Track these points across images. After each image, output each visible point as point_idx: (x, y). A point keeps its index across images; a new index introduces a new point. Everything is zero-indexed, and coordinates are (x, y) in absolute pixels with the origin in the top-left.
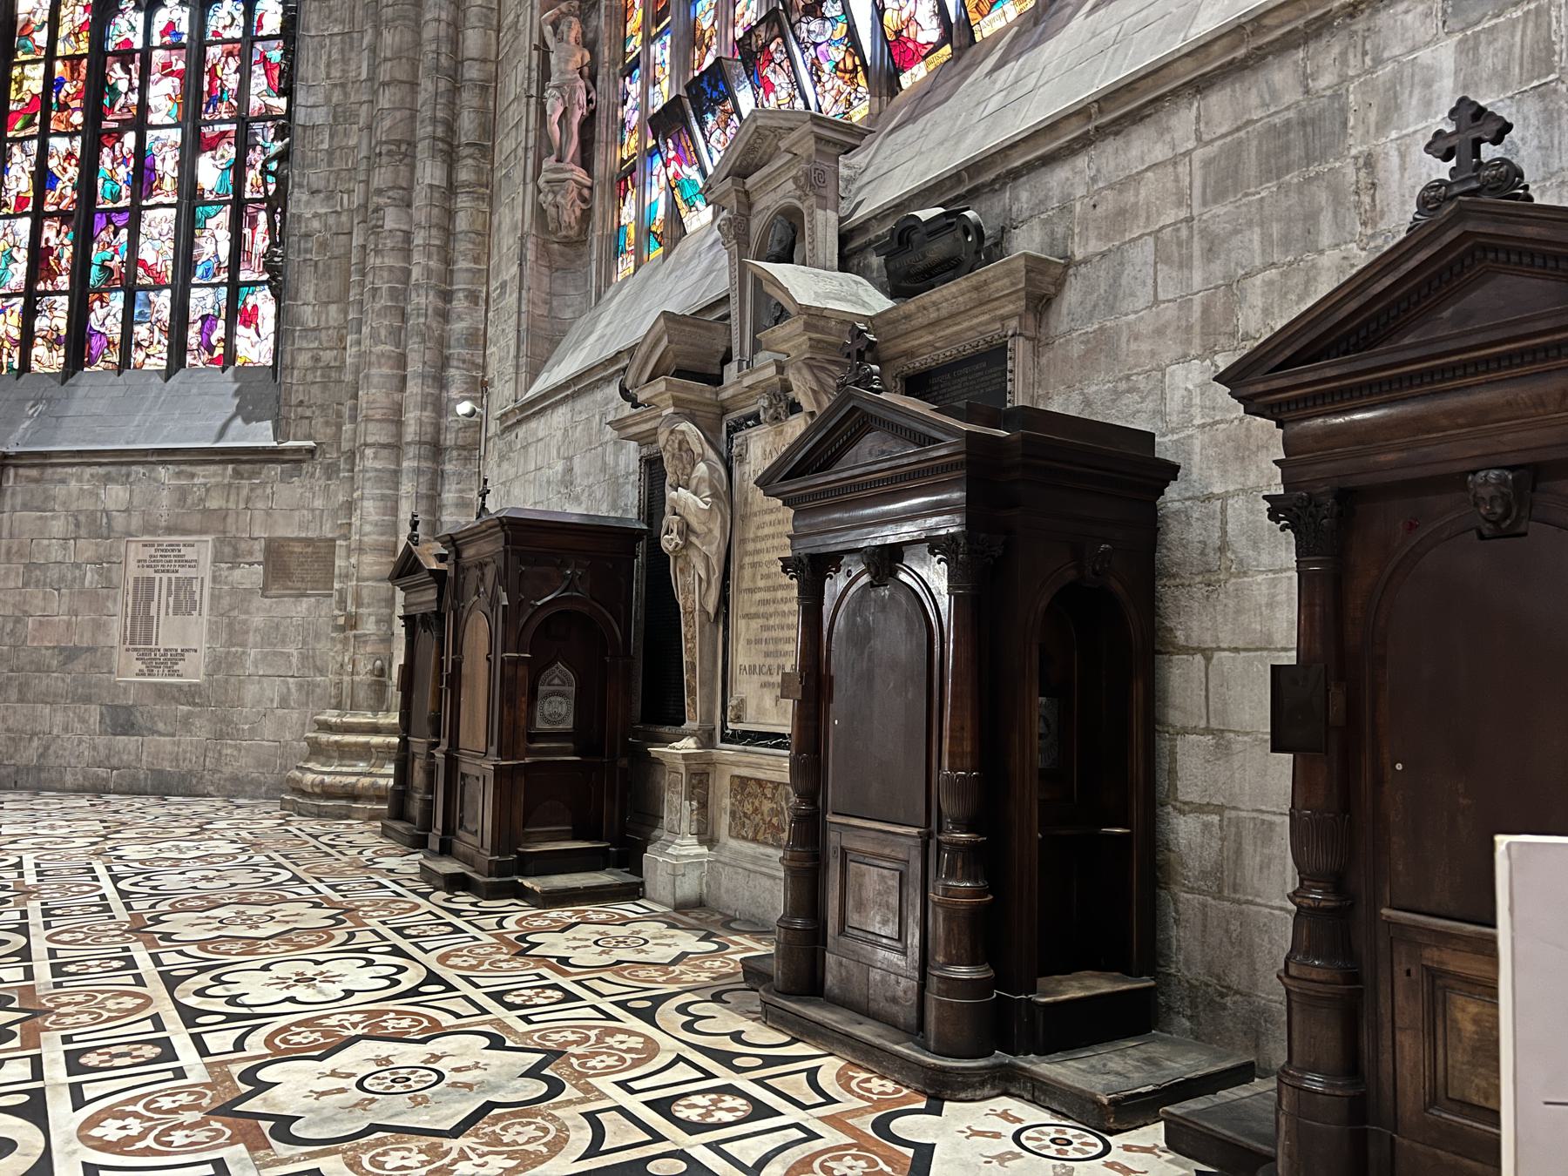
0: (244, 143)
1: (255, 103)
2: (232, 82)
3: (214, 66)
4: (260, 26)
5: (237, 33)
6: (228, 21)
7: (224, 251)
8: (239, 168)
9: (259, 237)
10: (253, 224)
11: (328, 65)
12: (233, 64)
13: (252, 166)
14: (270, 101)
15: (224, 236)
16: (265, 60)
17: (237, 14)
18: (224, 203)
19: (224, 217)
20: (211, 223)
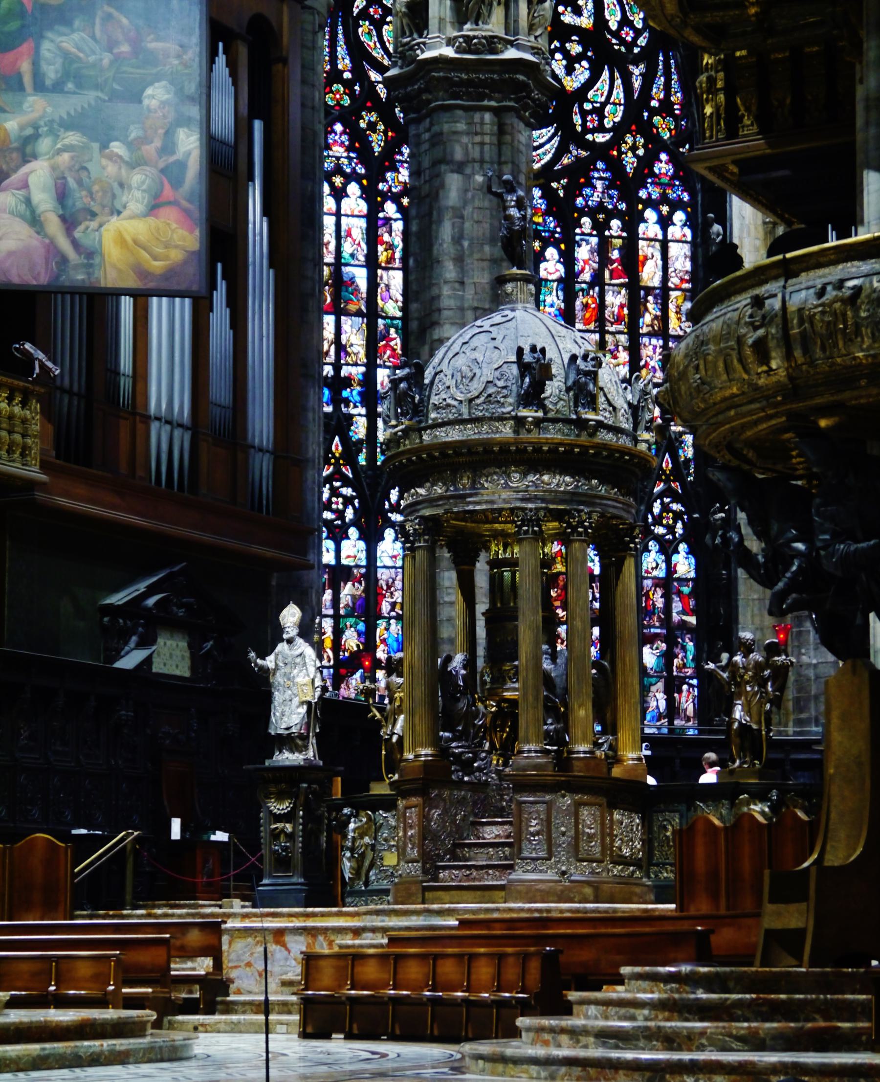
0: (671, 640)
1: (676, 617)
2: (660, 603)
3: (648, 592)
4: (676, 572)
5: (661, 573)
6: (654, 565)
7: (663, 705)
8: (668, 657)
9: (683, 699)
10: (680, 692)
11: (753, 616)
12: (659, 592)
13: (677, 657)
14: (685, 618)
15: (661, 697)
16: (679, 593)
17: (660, 562)
18: (661, 677)
19: (660, 685)
20: (653, 689)
